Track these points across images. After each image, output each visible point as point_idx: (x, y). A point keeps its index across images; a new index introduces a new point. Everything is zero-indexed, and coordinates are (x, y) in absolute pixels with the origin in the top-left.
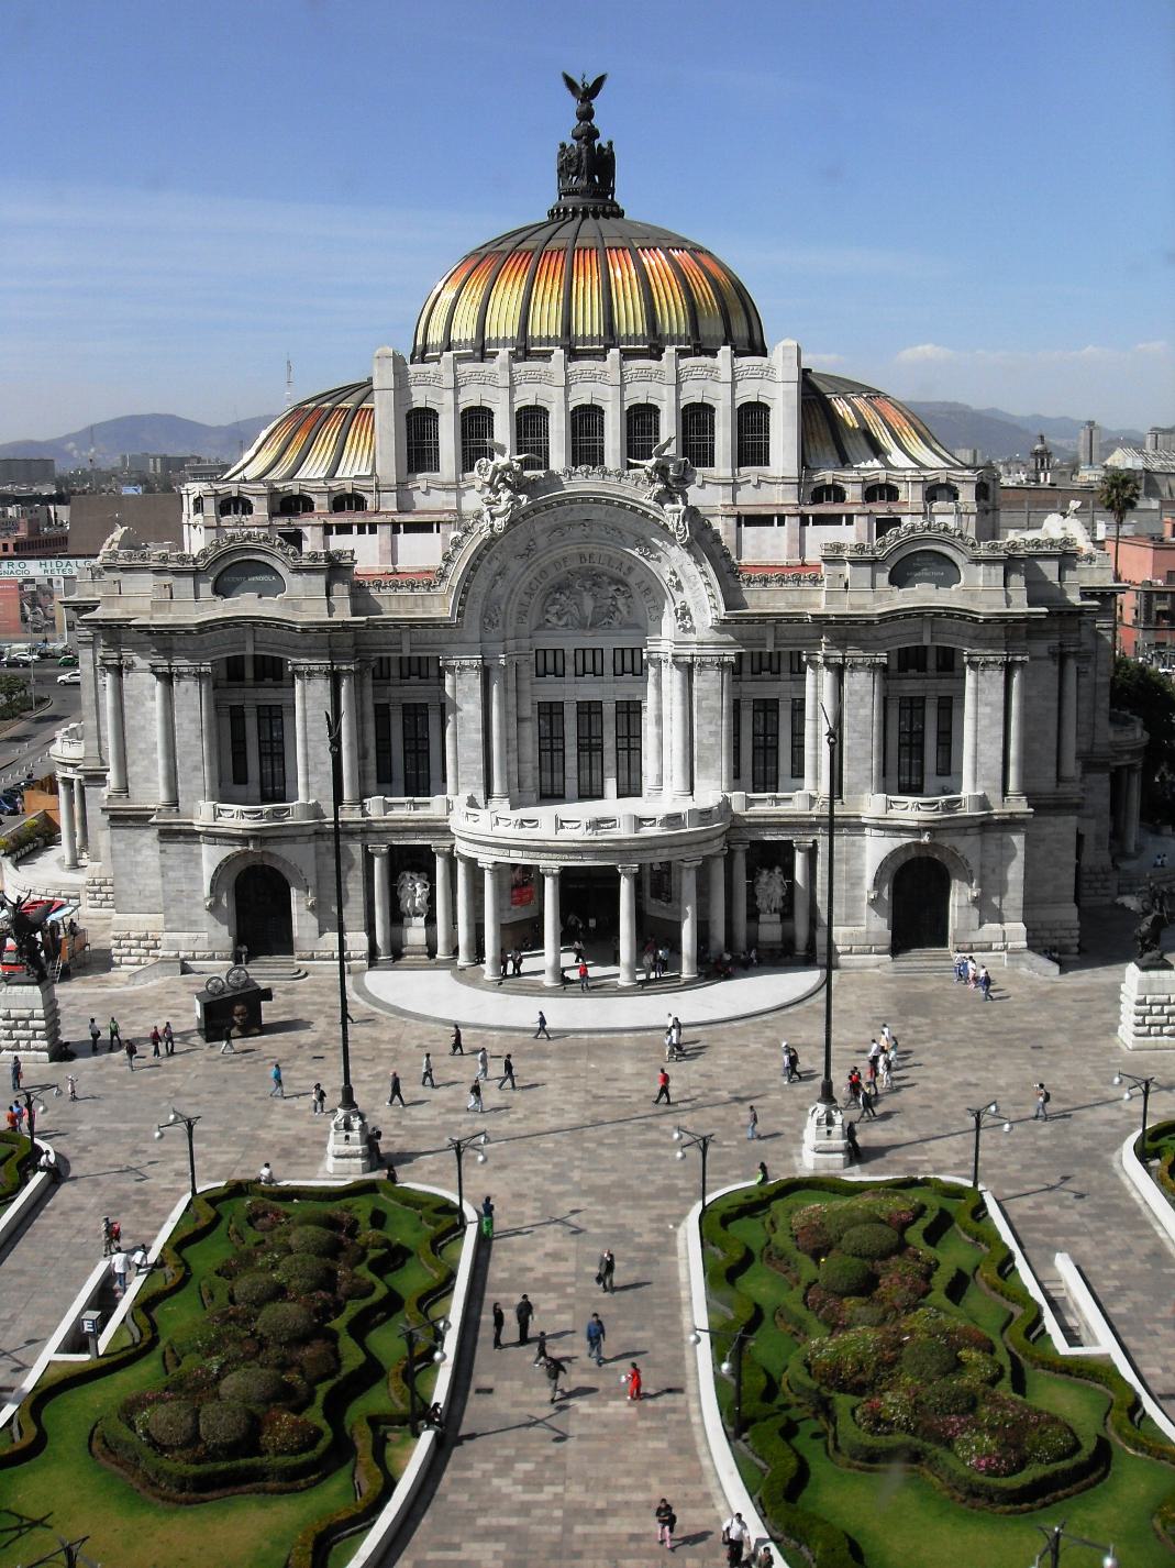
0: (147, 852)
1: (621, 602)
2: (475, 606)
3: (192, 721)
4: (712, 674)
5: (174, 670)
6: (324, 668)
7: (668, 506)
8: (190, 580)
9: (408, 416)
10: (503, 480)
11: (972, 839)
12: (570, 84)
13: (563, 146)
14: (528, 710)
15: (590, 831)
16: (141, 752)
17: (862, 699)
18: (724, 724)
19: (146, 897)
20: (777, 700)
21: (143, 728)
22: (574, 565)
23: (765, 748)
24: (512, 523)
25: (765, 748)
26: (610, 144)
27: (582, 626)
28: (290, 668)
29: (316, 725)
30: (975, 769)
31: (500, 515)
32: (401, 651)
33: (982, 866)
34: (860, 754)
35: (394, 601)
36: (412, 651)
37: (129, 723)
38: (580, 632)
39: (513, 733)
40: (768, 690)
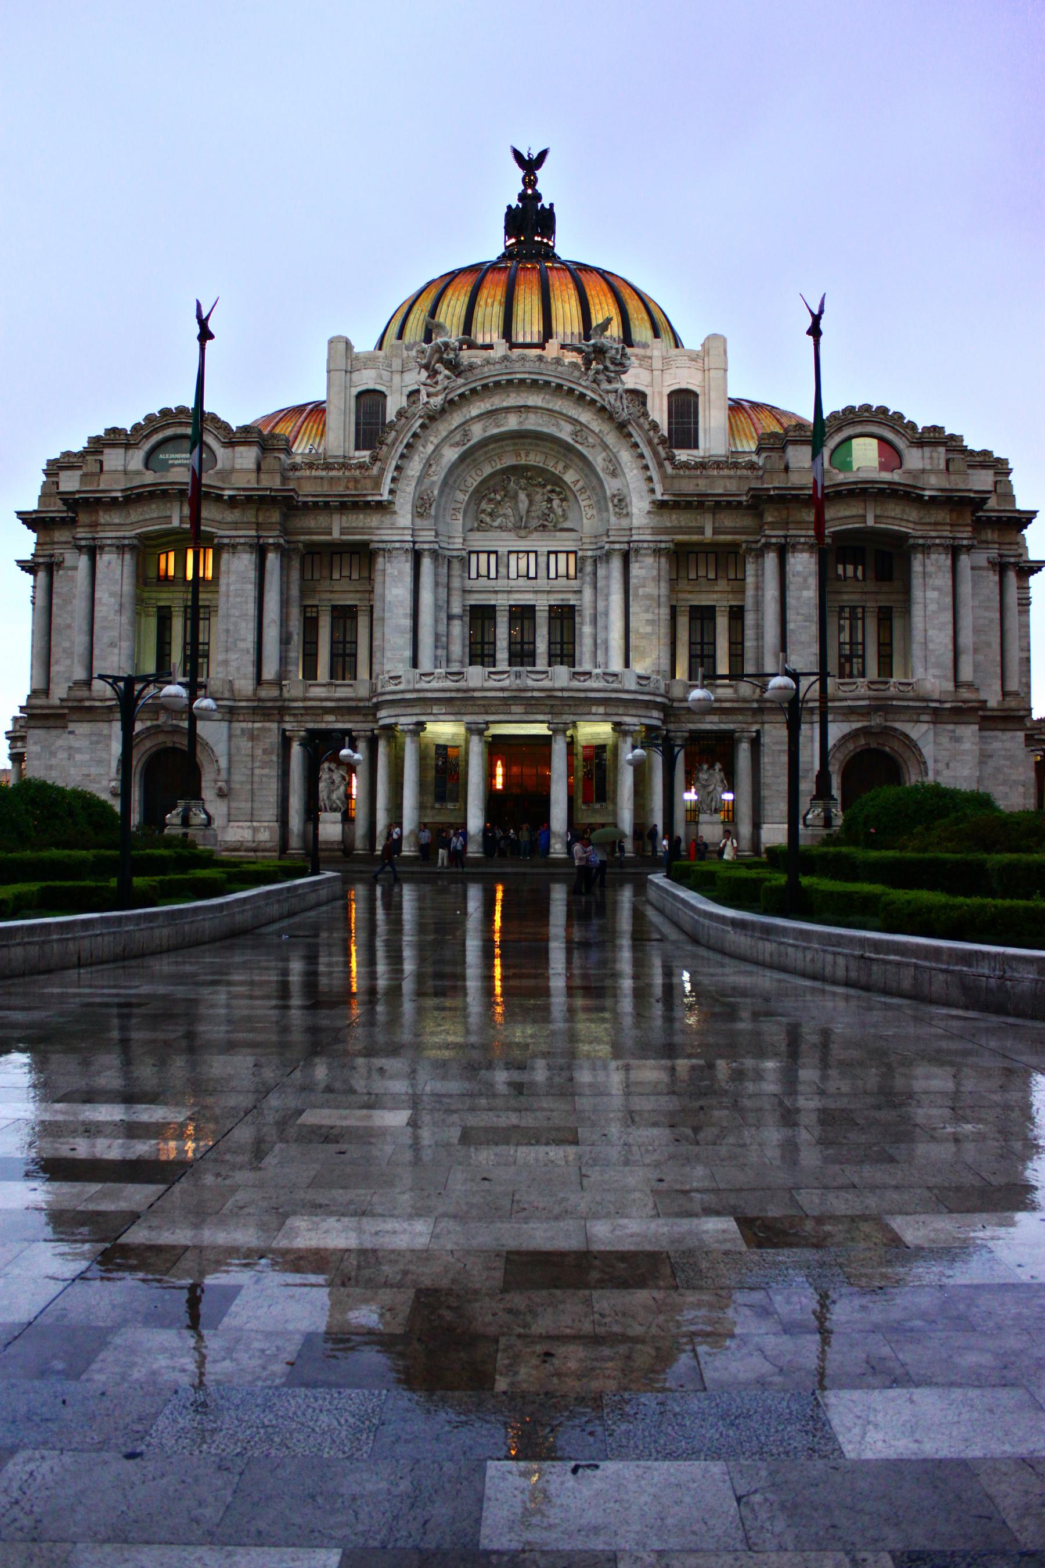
1: (556, 503)
3: (112, 594)
4: (650, 560)
5: (98, 543)
7: (605, 386)
8: (122, 451)
9: (360, 395)
10: (441, 360)
11: (924, 727)
13: (509, 207)
14: (456, 610)
15: (518, 681)
16: (65, 650)
17: (805, 580)
18: (664, 612)
20: (714, 607)
21: (69, 627)
23: (702, 656)
25: (702, 656)
26: (551, 205)
27: (517, 528)
28: (216, 541)
29: (238, 599)
30: (925, 657)
31: (436, 394)
32: (330, 534)
33: (936, 761)
34: (804, 638)
35: (326, 483)
37: (55, 620)
39: (442, 629)
40: (704, 600)
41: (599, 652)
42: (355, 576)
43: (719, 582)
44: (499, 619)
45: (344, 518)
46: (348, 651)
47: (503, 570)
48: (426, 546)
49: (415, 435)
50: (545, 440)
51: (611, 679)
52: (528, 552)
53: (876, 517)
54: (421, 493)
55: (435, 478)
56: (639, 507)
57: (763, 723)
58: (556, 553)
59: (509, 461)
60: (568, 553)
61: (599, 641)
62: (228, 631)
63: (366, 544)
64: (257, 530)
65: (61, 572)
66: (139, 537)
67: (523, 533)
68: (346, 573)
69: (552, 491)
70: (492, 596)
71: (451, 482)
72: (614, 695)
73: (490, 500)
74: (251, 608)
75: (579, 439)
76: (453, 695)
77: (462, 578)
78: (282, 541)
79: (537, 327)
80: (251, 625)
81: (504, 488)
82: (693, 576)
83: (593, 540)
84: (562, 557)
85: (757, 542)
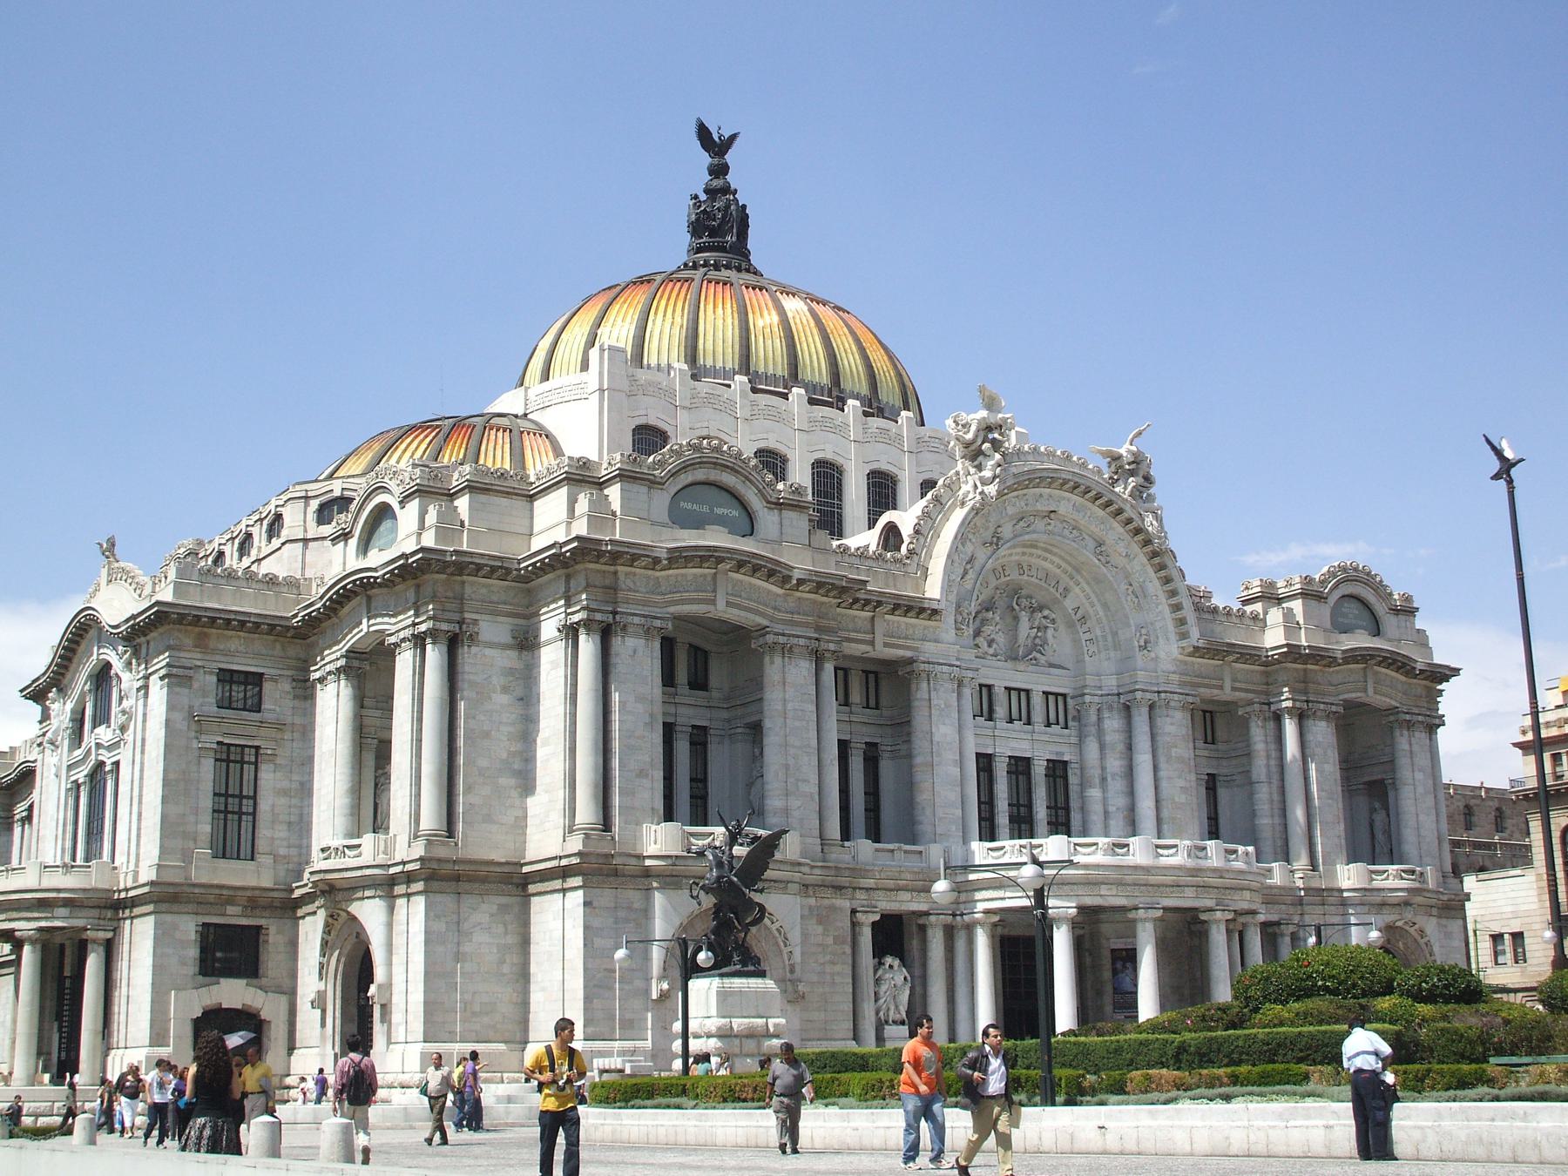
0: (480, 937)
1: (1050, 632)
4: (1178, 715)
6: (814, 644)
8: (644, 489)
11: (1434, 920)
12: (703, 133)
19: (474, 1014)
24: (1000, 494)
27: (1013, 657)
28: (770, 638)
29: (797, 724)
32: (872, 643)
38: (1009, 664)
41: (1112, 823)
56: (1169, 651)
59: (1014, 575)
61: (1112, 809)
62: (787, 767)
63: (911, 661)
64: (818, 629)
65: (474, 649)
79: (825, 379)
85: (1269, 704)
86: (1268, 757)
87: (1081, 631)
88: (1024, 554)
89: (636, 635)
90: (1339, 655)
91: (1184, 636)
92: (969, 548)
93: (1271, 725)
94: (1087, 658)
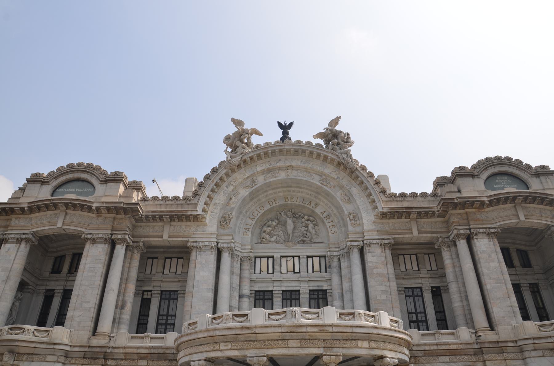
1: (311, 227)
2: (215, 211)
4: (379, 251)
6: (106, 236)
12: (280, 125)
14: (246, 291)
15: (293, 320)
17: (490, 256)
22: (283, 202)
27: (287, 241)
28: (83, 236)
29: (90, 274)
31: (235, 157)
32: (162, 237)
36: (169, 237)
39: (235, 303)
42: (179, 272)
43: (421, 271)
44: (275, 300)
45: (172, 227)
46: (169, 322)
47: (277, 268)
48: (225, 245)
49: (221, 179)
50: (304, 188)
51: (370, 319)
52: (293, 257)
53: (525, 215)
54: (225, 214)
55: (233, 206)
57: (485, 361)
58: (312, 257)
60: (320, 257)
64: (112, 231)
66: (34, 234)
67: (290, 244)
68: (173, 270)
69: (308, 220)
70: (270, 284)
71: (244, 211)
72: (375, 331)
73: (269, 226)
74: (99, 281)
75: (324, 183)
76: (238, 332)
77: (251, 273)
78: (127, 237)
80: (97, 292)
81: (278, 219)
82: (403, 269)
83: (337, 246)
84: (316, 260)
85: (448, 238)
86: (454, 267)
87: (326, 222)
88: (284, 191)
89: (12, 243)
90: (485, 199)
91: (376, 208)
92: (231, 188)
93: (453, 249)
94: (330, 234)
